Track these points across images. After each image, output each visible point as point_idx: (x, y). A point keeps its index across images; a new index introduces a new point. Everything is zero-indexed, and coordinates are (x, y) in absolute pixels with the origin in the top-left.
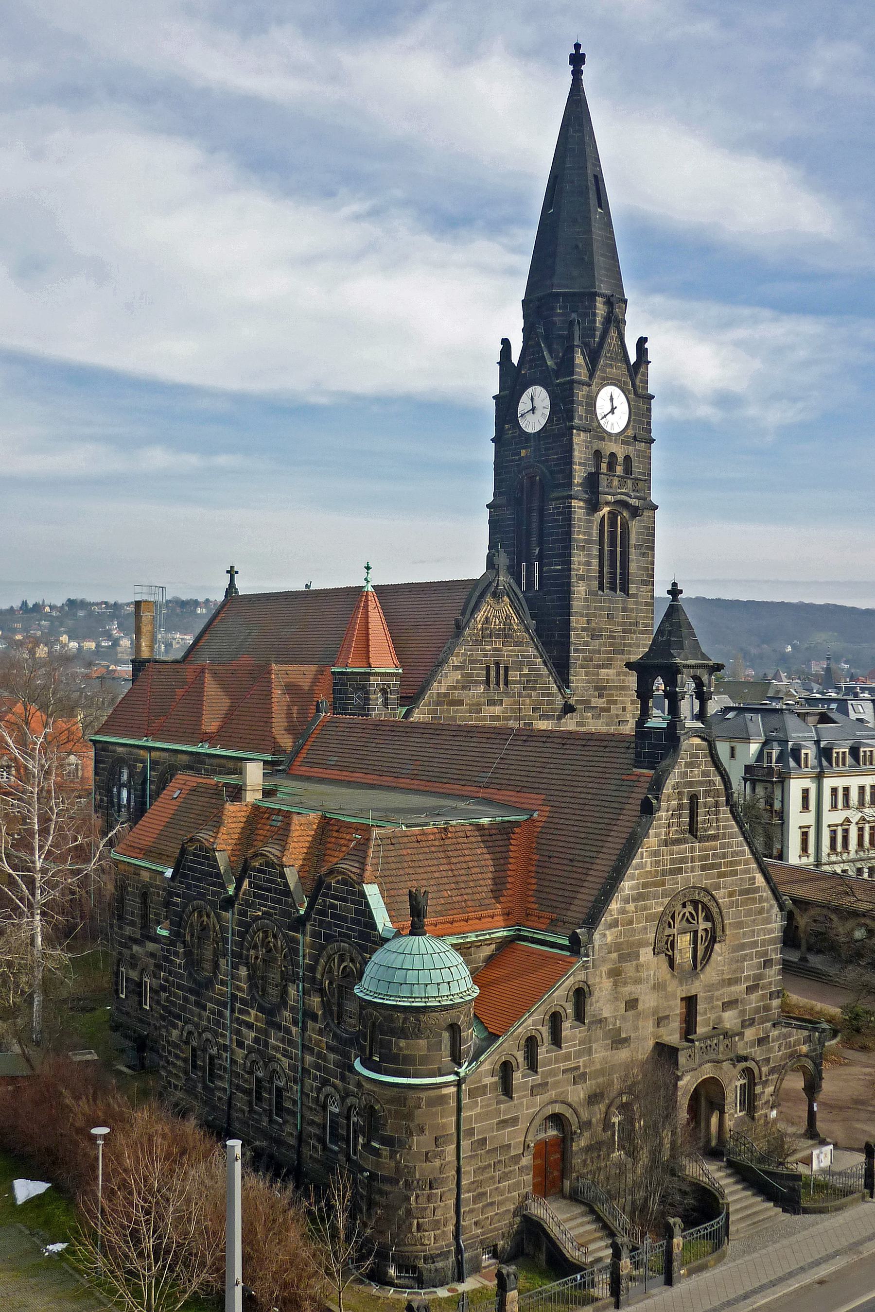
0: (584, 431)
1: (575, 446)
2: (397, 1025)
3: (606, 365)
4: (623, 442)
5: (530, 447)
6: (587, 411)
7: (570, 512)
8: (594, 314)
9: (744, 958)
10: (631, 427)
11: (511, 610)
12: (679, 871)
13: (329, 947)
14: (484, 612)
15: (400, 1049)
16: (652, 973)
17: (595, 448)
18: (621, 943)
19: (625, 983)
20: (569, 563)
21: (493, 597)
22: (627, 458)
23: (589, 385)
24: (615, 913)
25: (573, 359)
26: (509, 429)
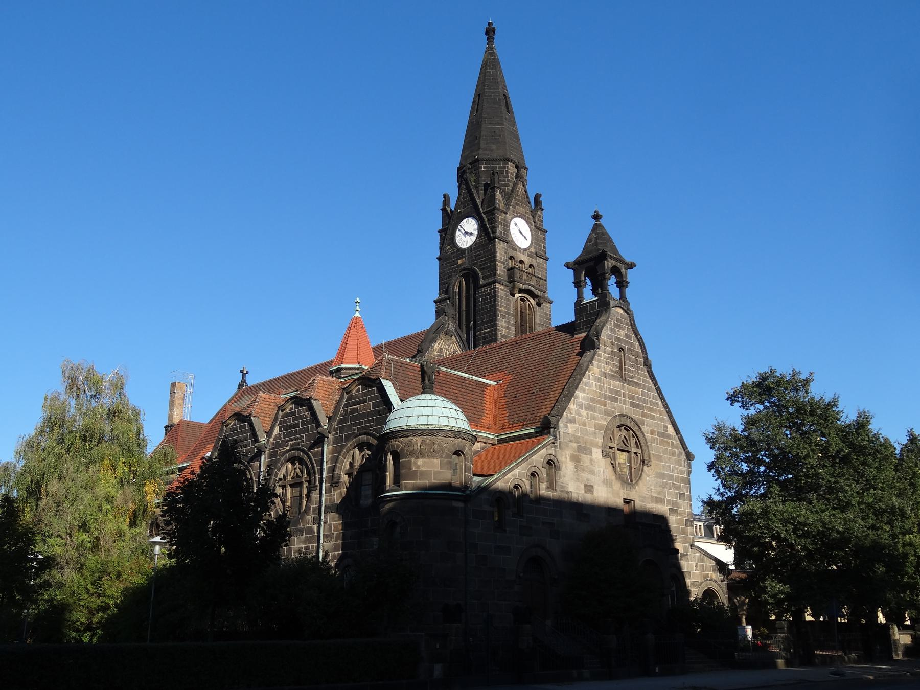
0: (504, 242)
1: (497, 250)
2: (416, 448)
3: (516, 204)
4: (528, 255)
6: (504, 229)
7: (495, 292)
8: (507, 172)
9: (665, 486)
10: (533, 247)
11: (457, 347)
12: (615, 400)
13: (349, 445)
14: (439, 344)
15: (418, 467)
16: (602, 470)
17: (510, 254)
18: (578, 438)
19: (583, 470)
20: (496, 325)
21: (446, 334)
22: (531, 266)
23: (506, 213)
24: (573, 412)
25: (494, 195)
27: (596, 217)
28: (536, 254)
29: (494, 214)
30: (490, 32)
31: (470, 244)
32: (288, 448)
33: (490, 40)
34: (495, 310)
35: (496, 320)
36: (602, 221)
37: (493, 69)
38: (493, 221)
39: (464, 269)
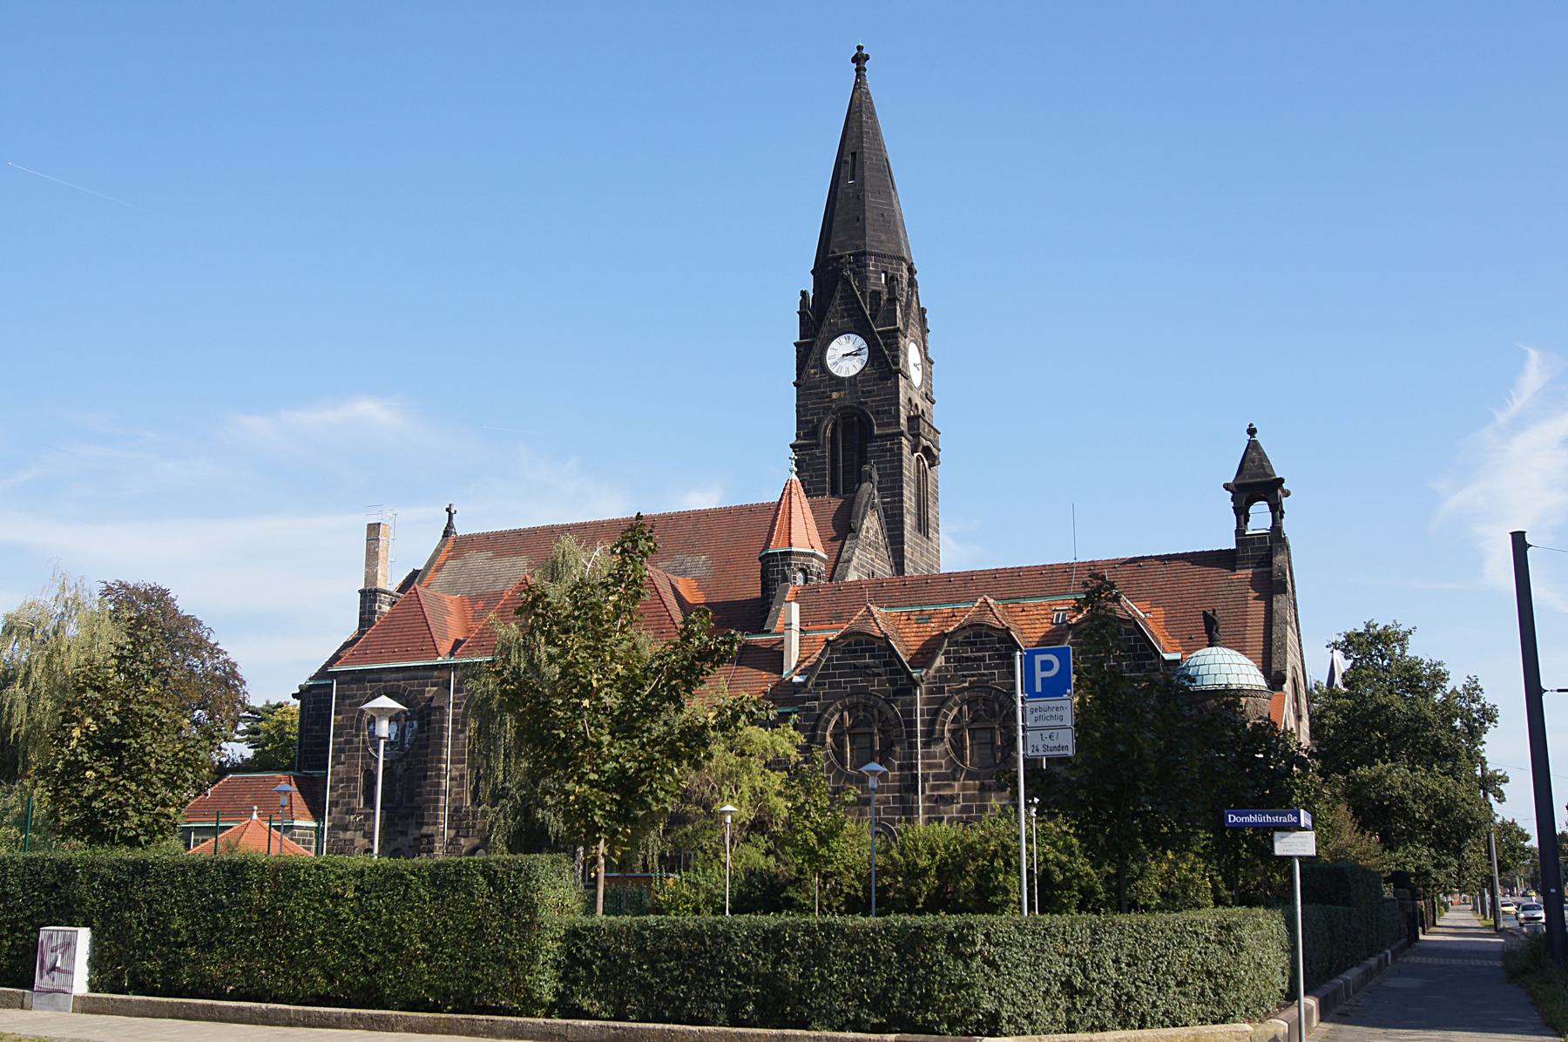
4: (921, 397)
5: (845, 390)
7: (901, 448)
8: (901, 276)
26: (815, 374)
27: (1252, 431)
28: (926, 395)
29: (897, 337)
30: (860, 59)
31: (853, 372)
32: (967, 685)
33: (862, 72)
34: (901, 473)
35: (901, 488)
36: (1257, 437)
37: (870, 118)
38: (894, 347)
39: (846, 407)
